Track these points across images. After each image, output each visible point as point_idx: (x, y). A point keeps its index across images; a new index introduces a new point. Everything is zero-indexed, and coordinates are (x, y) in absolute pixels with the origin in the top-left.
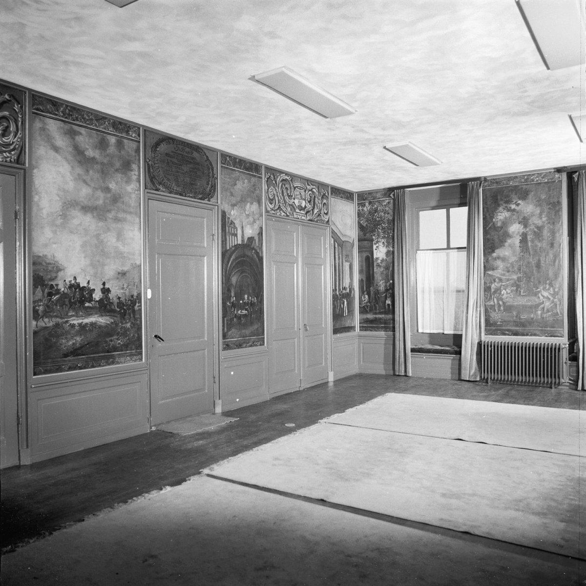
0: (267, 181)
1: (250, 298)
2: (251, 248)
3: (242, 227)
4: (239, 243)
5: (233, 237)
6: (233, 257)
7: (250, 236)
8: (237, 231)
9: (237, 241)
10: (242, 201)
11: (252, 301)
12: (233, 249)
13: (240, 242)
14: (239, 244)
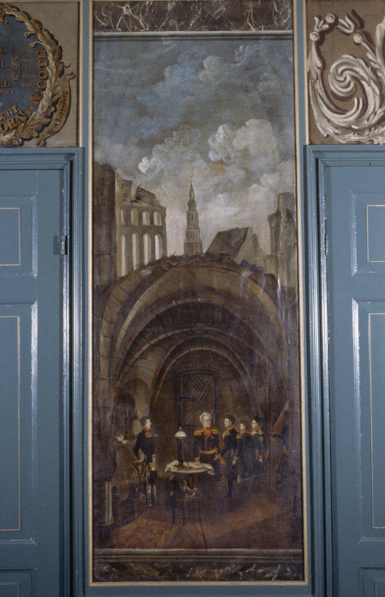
0: (319, 43)
1: (227, 422)
2: (234, 264)
3: (192, 204)
4: (170, 252)
5: (134, 237)
6: (146, 297)
7: (226, 226)
8: (163, 217)
9: (164, 246)
10: (197, 120)
11: (234, 432)
12: (146, 272)
13: (176, 246)
14: (174, 258)
